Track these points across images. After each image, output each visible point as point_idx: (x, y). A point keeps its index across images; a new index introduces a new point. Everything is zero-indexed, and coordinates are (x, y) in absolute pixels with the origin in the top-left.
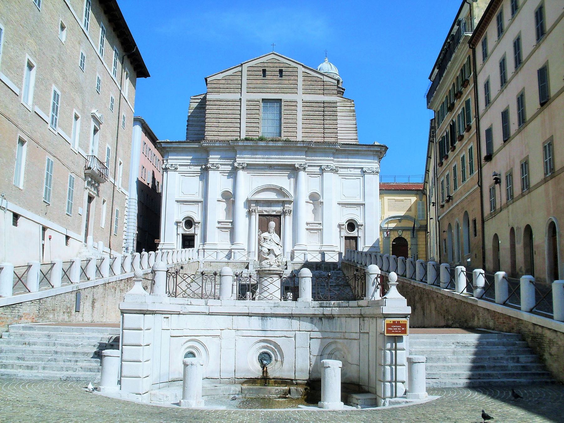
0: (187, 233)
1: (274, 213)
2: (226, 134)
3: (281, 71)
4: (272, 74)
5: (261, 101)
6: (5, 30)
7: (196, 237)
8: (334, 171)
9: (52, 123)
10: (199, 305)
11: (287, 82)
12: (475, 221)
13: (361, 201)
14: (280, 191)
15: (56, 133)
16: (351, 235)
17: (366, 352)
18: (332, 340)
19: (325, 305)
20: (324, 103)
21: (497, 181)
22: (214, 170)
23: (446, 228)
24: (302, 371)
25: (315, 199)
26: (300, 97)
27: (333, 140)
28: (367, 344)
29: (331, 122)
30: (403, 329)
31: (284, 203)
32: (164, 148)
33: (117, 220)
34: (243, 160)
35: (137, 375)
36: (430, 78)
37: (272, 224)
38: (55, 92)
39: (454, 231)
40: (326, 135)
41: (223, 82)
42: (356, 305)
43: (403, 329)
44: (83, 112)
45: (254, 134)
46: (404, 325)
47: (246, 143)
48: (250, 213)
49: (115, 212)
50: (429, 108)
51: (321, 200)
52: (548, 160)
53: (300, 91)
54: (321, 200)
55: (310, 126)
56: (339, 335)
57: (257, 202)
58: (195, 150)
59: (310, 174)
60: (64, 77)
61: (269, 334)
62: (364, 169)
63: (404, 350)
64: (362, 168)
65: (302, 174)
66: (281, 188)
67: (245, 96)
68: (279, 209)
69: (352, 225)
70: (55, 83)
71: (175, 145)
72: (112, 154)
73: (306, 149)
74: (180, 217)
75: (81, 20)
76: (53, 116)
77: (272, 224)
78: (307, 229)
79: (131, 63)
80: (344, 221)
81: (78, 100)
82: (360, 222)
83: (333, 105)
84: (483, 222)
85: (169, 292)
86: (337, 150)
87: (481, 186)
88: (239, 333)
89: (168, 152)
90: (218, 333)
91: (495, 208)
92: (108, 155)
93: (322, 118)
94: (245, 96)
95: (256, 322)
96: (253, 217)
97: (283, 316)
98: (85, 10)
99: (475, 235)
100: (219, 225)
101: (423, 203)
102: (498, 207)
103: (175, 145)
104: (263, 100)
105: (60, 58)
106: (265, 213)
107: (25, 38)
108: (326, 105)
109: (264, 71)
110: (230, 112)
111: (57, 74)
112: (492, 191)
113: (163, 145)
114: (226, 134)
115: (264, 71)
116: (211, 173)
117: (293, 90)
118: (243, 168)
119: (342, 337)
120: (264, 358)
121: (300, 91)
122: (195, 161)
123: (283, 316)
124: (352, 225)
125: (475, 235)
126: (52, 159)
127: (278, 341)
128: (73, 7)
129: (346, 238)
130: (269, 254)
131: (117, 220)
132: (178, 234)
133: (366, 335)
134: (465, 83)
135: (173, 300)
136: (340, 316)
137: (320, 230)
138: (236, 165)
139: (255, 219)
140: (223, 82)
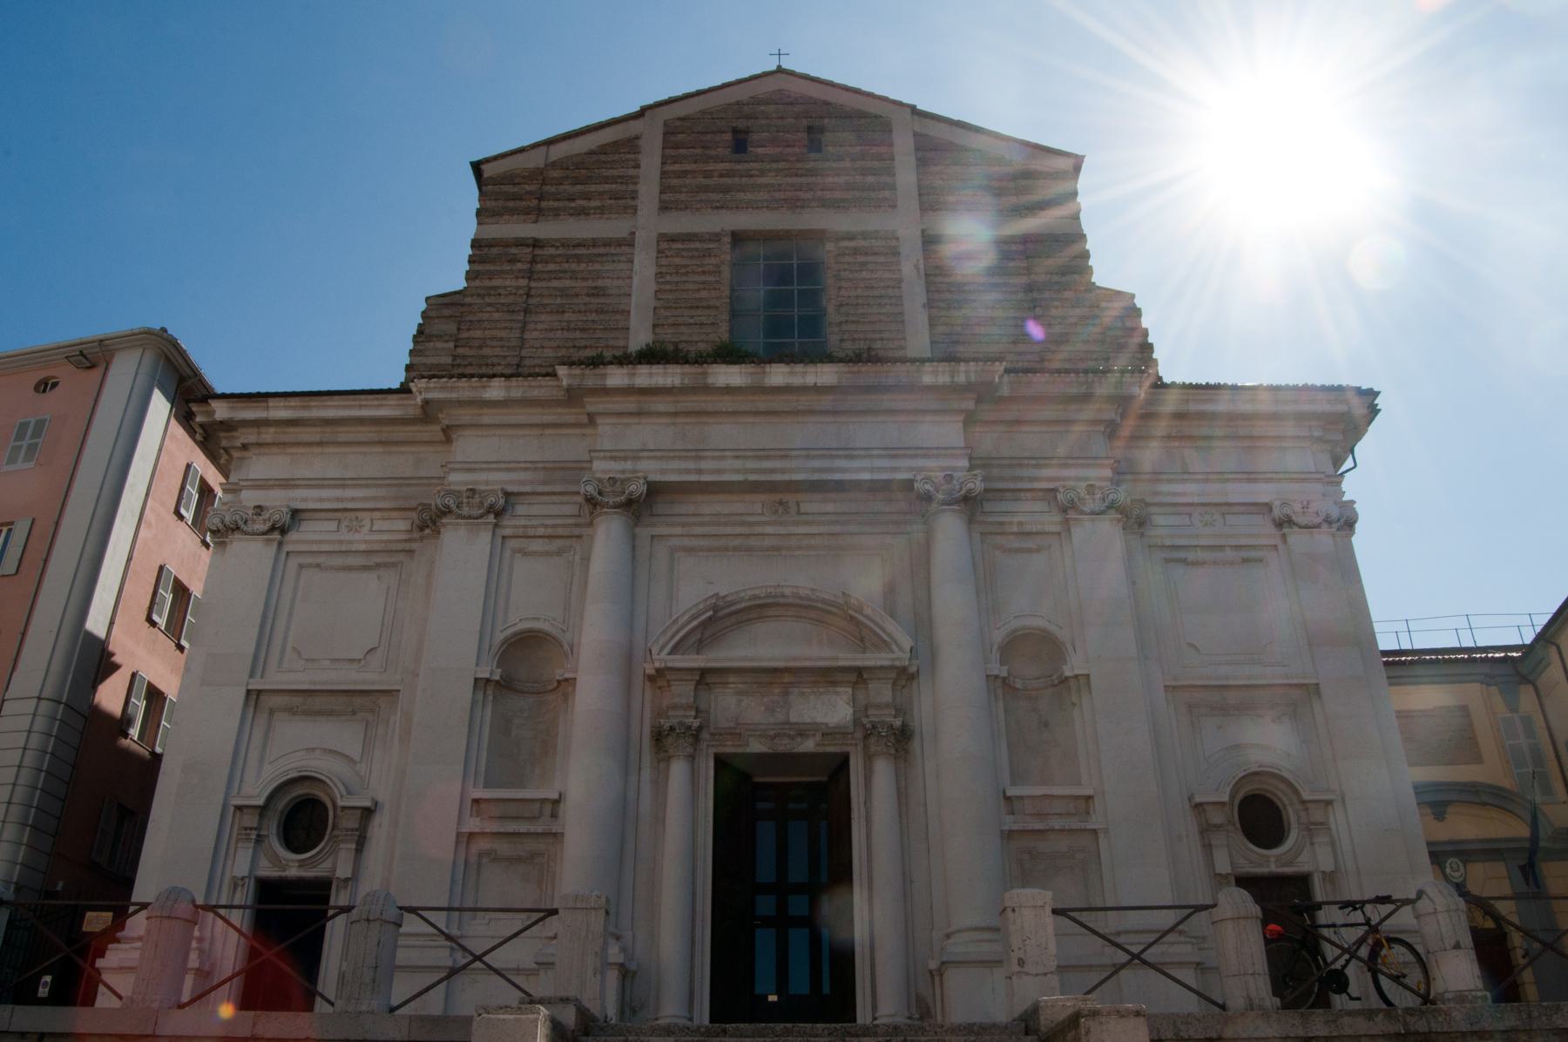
0: (293, 872)
1: (809, 746)
5: (727, 239)
16: (1273, 868)
31: (860, 676)
32: (229, 426)
34: (629, 465)
41: (556, 174)
47: (647, 376)
51: (1074, 666)
54: (1074, 666)
57: (705, 678)
62: (1277, 513)
64: (1268, 507)
71: (279, 411)
73: (970, 405)
78: (1009, 835)
94: (648, 222)
96: (678, 771)
100: (473, 824)
101: (1527, 722)
103: (279, 411)
104: (738, 238)
106: (756, 747)
113: (221, 411)
122: (382, 492)
137: (1095, 832)
138: (590, 489)
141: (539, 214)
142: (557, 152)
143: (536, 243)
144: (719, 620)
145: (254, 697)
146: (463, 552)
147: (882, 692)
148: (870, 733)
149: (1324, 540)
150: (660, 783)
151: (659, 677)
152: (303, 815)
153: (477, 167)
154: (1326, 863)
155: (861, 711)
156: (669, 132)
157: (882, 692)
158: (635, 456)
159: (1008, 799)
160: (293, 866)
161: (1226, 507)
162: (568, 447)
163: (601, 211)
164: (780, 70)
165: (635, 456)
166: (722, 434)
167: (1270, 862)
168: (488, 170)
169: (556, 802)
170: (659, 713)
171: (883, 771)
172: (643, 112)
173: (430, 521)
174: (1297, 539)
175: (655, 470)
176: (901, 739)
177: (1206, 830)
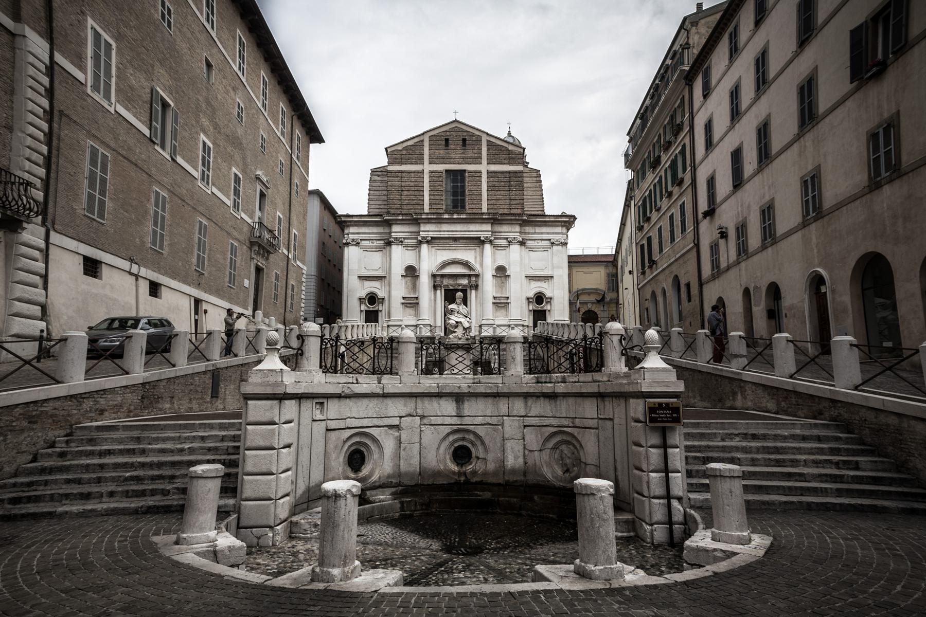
2: (409, 207)
3: (464, 140)
4: (455, 145)
6: (117, 47)
7: (380, 314)
8: (522, 243)
9: (203, 179)
10: (367, 384)
11: (470, 152)
12: (688, 285)
13: (549, 273)
14: (466, 264)
15: (209, 192)
17: (611, 447)
18: (555, 429)
19: (543, 380)
20: (510, 172)
21: (724, 235)
22: (397, 244)
23: (648, 296)
24: (513, 471)
25: (501, 272)
26: (484, 167)
27: (519, 211)
28: (611, 436)
29: (517, 193)
30: (675, 415)
31: (469, 276)
33: (292, 296)
35: (266, 496)
36: (628, 134)
37: (459, 294)
38: (204, 144)
39: (660, 299)
40: (513, 207)
41: (404, 152)
42: (590, 379)
43: (675, 415)
44: (244, 171)
45: (438, 206)
46: (676, 410)
48: (435, 287)
49: (290, 287)
50: (626, 167)
52: (810, 197)
53: (484, 161)
55: (495, 198)
56: (565, 422)
57: (443, 276)
58: (376, 224)
59: (495, 247)
60: (216, 127)
61: (467, 420)
63: (677, 447)
65: (487, 247)
66: (467, 262)
67: (427, 167)
68: (465, 282)
69: (539, 298)
70: (205, 133)
72: (284, 225)
74: (363, 294)
75: (234, 62)
76: (203, 172)
77: (459, 294)
79: (303, 126)
80: (531, 294)
81: (237, 157)
82: (548, 294)
83: (519, 175)
84: (701, 285)
85: (326, 367)
86: (524, 221)
87: (697, 246)
88: (425, 421)
89: (348, 226)
90: (396, 421)
91: (718, 267)
92: (280, 223)
93: (507, 188)
94: (427, 167)
95: (448, 407)
96: (438, 292)
97: (486, 395)
98: (238, 50)
99: (689, 300)
100: (403, 301)
102: (723, 265)
105: (208, 103)
107: (153, 66)
108: (512, 175)
109: (447, 140)
110: (412, 184)
111: (205, 122)
112: (714, 248)
113: (343, 219)
114: (409, 207)
115: (447, 140)
116: (394, 247)
117: (477, 160)
118: (428, 242)
119: (571, 425)
120: (461, 454)
121: (484, 161)
123: (486, 395)
124: (539, 298)
125: (689, 300)
126: (204, 222)
127: (481, 431)
128: (221, 43)
129: (534, 311)
130: (456, 327)
131: (292, 296)
132: (361, 311)
133: (609, 423)
134: (678, 129)
135: (331, 378)
136: (566, 395)
138: (420, 238)
139: (440, 294)
140: (404, 152)
141: (401, 163)
142: (405, 145)
143: (402, 172)
144: (445, 265)
145: (360, 277)
146: (396, 250)
147: (473, 279)
148: (471, 286)
149: (560, 248)
150: (435, 294)
151: (434, 276)
152: (372, 298)
153: (386, 149)
154: (549, 308)
155: (470, 282)
156: (431, 138)
157: (473, 279)
158: (428, 231)
159: (495, 298)
160: (371, 308)
161: (542, 240)
162: (413, 228)
163: (416, 163)
164: (456, 121)
165: (428, 231)
166: (445, 227)
167: (539, 307)
168: (389, 150)
169: (417, 298)
170: (435, 282)
171: (473, 292)
172: (423, 134)
173: (389, 243)
174: (555, 248)
175: (431, 234)
176: (476, 287)
177: (529, 302)
